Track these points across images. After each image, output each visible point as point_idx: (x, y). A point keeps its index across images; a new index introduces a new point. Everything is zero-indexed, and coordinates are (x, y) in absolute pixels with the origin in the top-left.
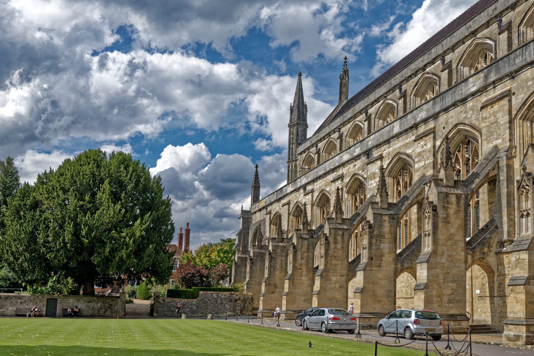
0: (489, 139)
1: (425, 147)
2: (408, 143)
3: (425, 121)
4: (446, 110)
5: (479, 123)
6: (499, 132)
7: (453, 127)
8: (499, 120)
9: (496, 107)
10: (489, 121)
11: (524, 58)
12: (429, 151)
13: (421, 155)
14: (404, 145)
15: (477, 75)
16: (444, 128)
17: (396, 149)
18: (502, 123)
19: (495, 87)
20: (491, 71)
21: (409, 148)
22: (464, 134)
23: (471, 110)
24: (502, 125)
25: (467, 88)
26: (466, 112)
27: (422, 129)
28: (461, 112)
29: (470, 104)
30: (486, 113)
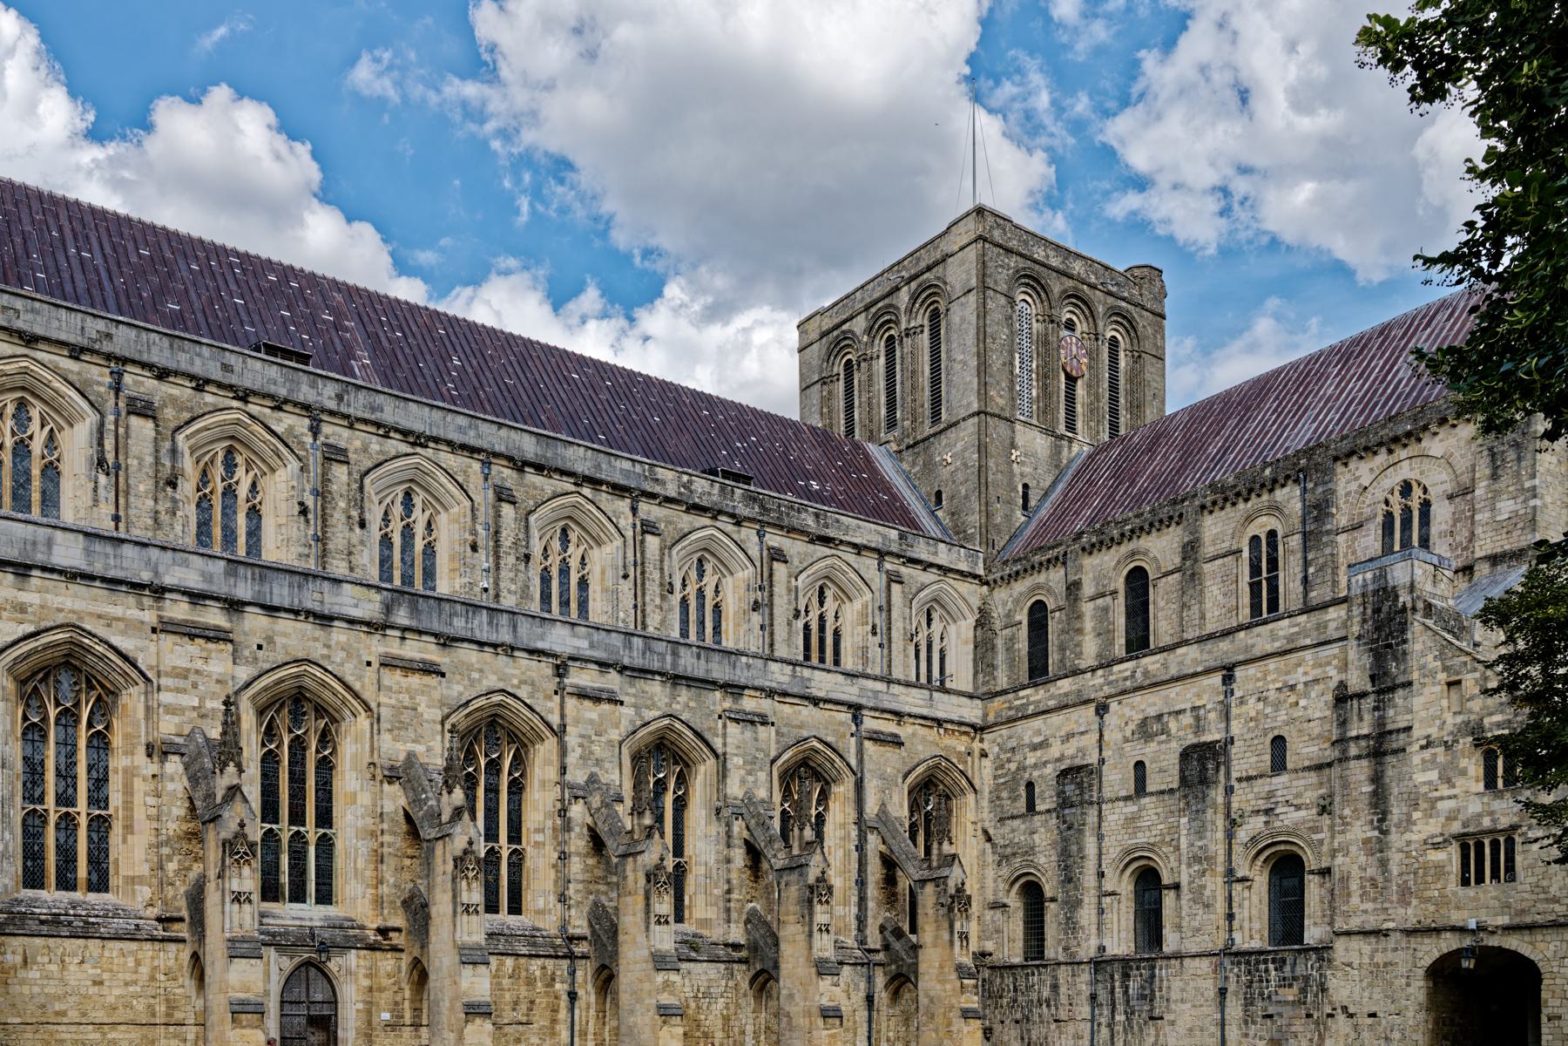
0: (396, 732)
1: (199, 664)
2: (118, 619)
3: (196, 598)
4: (271, 610)
5: (363, 686)
6: (419, 731)
7: (295, 661)
8: (420, 709)
9: (415, 680)
10: (398, 700)
11: (470, 626)
12: (218, 681)
13: (186, 678)
14: (100, 617)
15: (364, 590)
16: (260, 647)
17: (60, 610)
18: (426, 716)
19: (403, 638)
20: (400, 605)
21: (123, 633)
22: (304, 684)
23: (343, 649)
24: (427, 721)
25: (338, 600)
26: (328, 647)
27: (179, 610)
28: (316, 639)
29: (340, 634)
30: (393, 678)
